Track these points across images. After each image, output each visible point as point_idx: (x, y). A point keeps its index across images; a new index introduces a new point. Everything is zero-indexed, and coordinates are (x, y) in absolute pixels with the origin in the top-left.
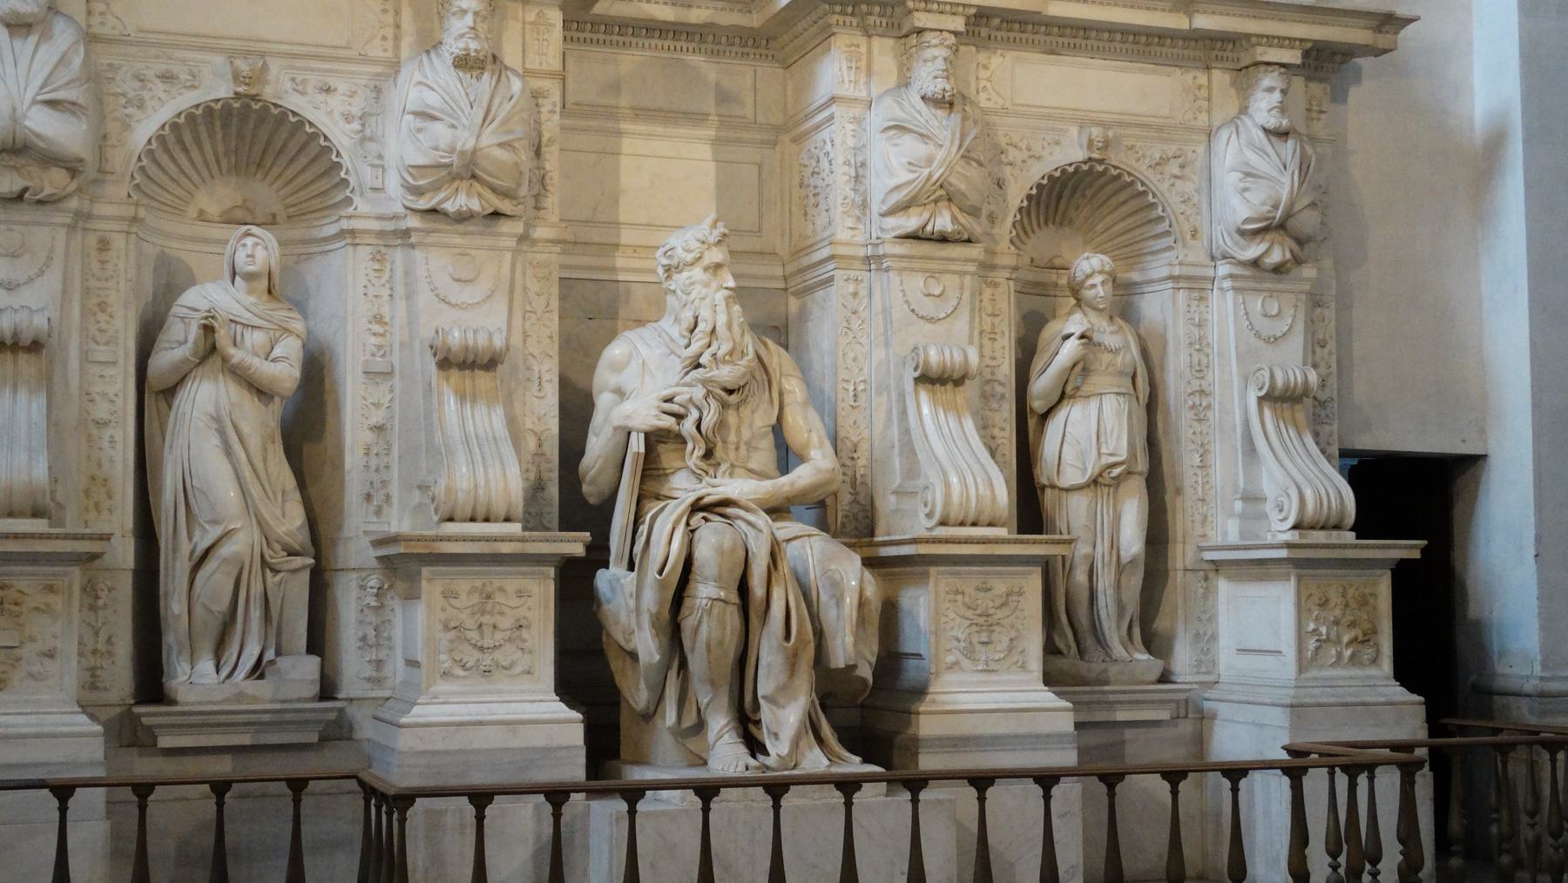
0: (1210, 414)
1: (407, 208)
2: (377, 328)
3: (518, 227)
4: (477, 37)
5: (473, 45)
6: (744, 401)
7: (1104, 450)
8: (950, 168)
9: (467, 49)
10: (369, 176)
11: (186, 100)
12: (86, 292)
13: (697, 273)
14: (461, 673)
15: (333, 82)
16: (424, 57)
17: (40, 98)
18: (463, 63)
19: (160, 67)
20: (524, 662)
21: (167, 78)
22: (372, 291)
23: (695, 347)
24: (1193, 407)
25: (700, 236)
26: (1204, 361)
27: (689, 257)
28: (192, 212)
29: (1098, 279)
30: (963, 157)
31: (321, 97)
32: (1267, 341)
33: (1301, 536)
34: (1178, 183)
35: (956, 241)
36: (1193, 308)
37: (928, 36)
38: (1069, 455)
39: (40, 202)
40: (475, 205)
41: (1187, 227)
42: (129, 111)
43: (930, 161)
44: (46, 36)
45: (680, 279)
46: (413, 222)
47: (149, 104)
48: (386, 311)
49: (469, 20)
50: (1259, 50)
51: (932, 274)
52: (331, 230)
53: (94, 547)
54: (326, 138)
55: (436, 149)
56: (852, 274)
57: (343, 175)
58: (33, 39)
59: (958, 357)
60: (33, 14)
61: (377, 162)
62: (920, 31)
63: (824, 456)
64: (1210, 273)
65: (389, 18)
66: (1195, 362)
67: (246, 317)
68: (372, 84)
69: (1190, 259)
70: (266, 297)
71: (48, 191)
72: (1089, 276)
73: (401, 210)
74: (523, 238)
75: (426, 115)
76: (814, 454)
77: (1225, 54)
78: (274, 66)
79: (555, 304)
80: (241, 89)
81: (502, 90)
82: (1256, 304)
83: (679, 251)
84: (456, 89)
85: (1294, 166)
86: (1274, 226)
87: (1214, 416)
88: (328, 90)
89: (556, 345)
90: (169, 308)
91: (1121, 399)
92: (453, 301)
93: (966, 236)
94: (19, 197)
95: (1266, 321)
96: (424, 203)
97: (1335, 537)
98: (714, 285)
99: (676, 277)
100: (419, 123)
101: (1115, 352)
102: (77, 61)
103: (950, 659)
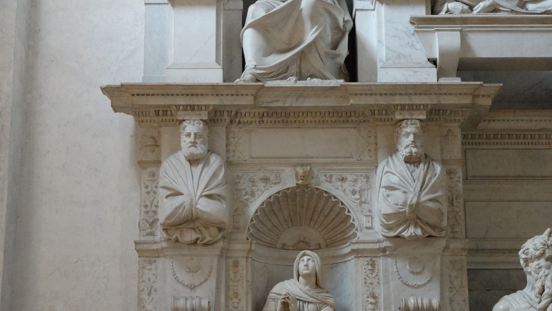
1: (384, 236)
2: (371, 300)
3: (443, 243)
4: (415, 146)
5: (414, 150)
9: (411, 152)
10: (365, 222)
11: (273, 190)
12: (228, 288)
13: (542, 262)
15: (345, 175)
16: (389, 158)
17: (204, 194)
18: (409, 160)
19: (261, 175)
21: (266, 180)
22: (369, 281)
23: (544, 303)
25: (542, 241)
27: (538, 253)
28: (279, 245)
31: (339, 183)
39: (205, 245)
40: (419, 232)
42: (247, 197)
44: (207, 164)
45: (533, 265)
47: (256, 193)
48: (377, 292)
49: (411, 138)
52: (348, 250)
54: (342, 204)
55: (397, 205)
57: (351, 221)
58: (200, 166)
60: (201, 154)
61: (368, 214)
65: (372, 140)
67: (305, 297)
68: (364, 174)
70: (314, 286)
71: (208, 239)
73: (381, 238)
74: (446, 248)
75: (391, 188)
78: (315, 170)
79: (466, 283)
80: (300, 182)
81: (430, 172)
83: (531, 250)
84: (407, 174)
88: (343, 180)
89: (468, 306)
90: (268, 294)
92: (410, 284)
94: (195, 243)
96: (392, 234)
99: (530, 264)
100: (389, 192)
102: (221, 175)
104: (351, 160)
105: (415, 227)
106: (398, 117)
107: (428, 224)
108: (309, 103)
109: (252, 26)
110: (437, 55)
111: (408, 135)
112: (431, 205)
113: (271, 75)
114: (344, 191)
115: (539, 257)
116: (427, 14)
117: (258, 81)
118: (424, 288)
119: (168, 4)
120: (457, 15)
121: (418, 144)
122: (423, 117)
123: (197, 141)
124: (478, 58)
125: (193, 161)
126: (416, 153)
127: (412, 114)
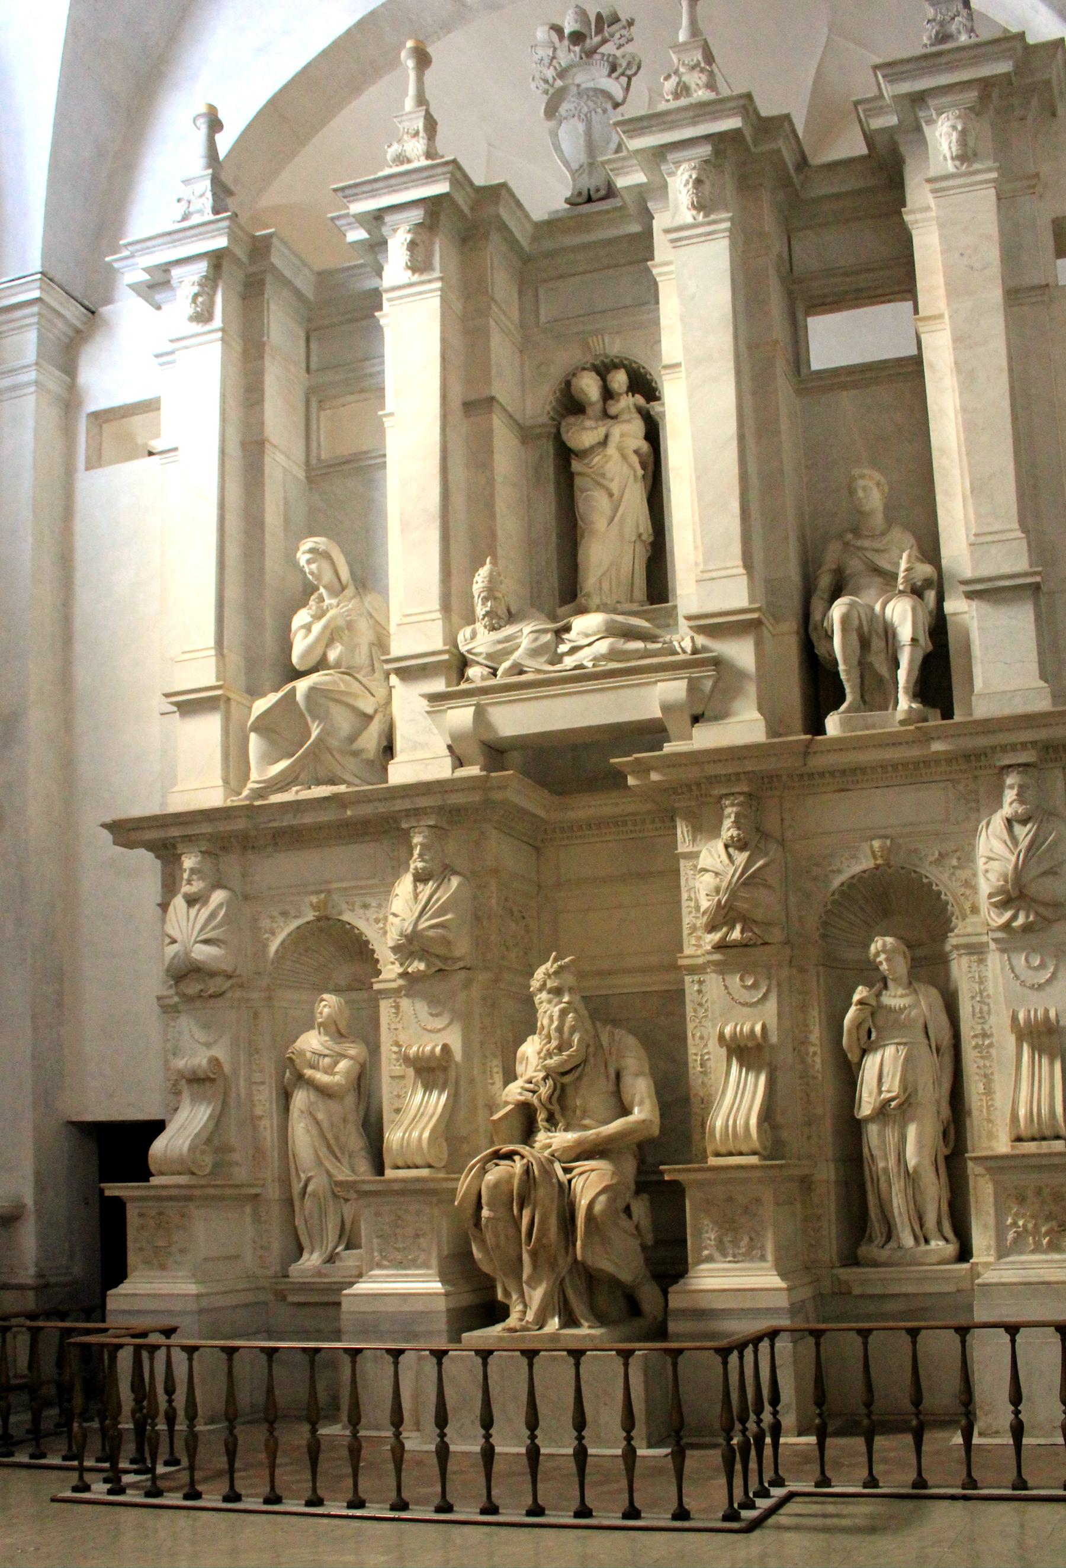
0: (991, 1050)
5: (420, 865)
6: (579, 1078)
7: (883, 1089)
8: (733, 893)
9: (416, 869)
13: (544, 995)
14: (386, 1263)
20: (423, 1257)
24: (975, 1047)
26: (985, 1008)
29: (882, 957)
30: (744, 884)
32: (1032, 987)
33: (1013, 1147)
34: (958, 872)
35: (755, 945)
36: (974, 968)
37: (723, 801)
38: (865, 1095)
40: (422, 966)
41: (967, 906)
43: (717, 890)
46: (401, 982)
50: (997, 756)
51: (745, 970)
53: (257, 1190)
56: (696, 978)
58: (197, 907)
59: (746, 1029)
60: (195, 893)
62: (721, 797)
63: (640, 1112)
64: (984, 939)
66: (977, 1010)
69: (969, 930)
72: (877, 954)
76: (636, 1110)
77: (982, 764)
82: (1020, 960)
85: (1024, 844)
86: (1013, 895)
87: (994, 1052)
91: (901, 1048)
93: (759, 942)
95: (1030, 972)
97: (1045, 1147)
98: (555, 1000)
101: (902, 1010)
102: (222, 913)
103: (706, 1253)
104: (370, 882)
105: (420, 960)
106: (404, 826)
107: (438, 956)
108: (308, 819)
109: (255, 728)
110: (450, 743)
111: (416, 845)
112: (431, 933)
113: (275, 788)
114: (368, 920)
115: (540, 990)
116: (448, 685)
117: (262, 797)
118: (443, 1032)
119: (174, 712)
120: (479, 684)
121: (427, 857)
122: (431, 823)
123: (194, 877)
124: (507, 738)
125: (192, 901)
126: (423, 869)
127: (418, 821)
